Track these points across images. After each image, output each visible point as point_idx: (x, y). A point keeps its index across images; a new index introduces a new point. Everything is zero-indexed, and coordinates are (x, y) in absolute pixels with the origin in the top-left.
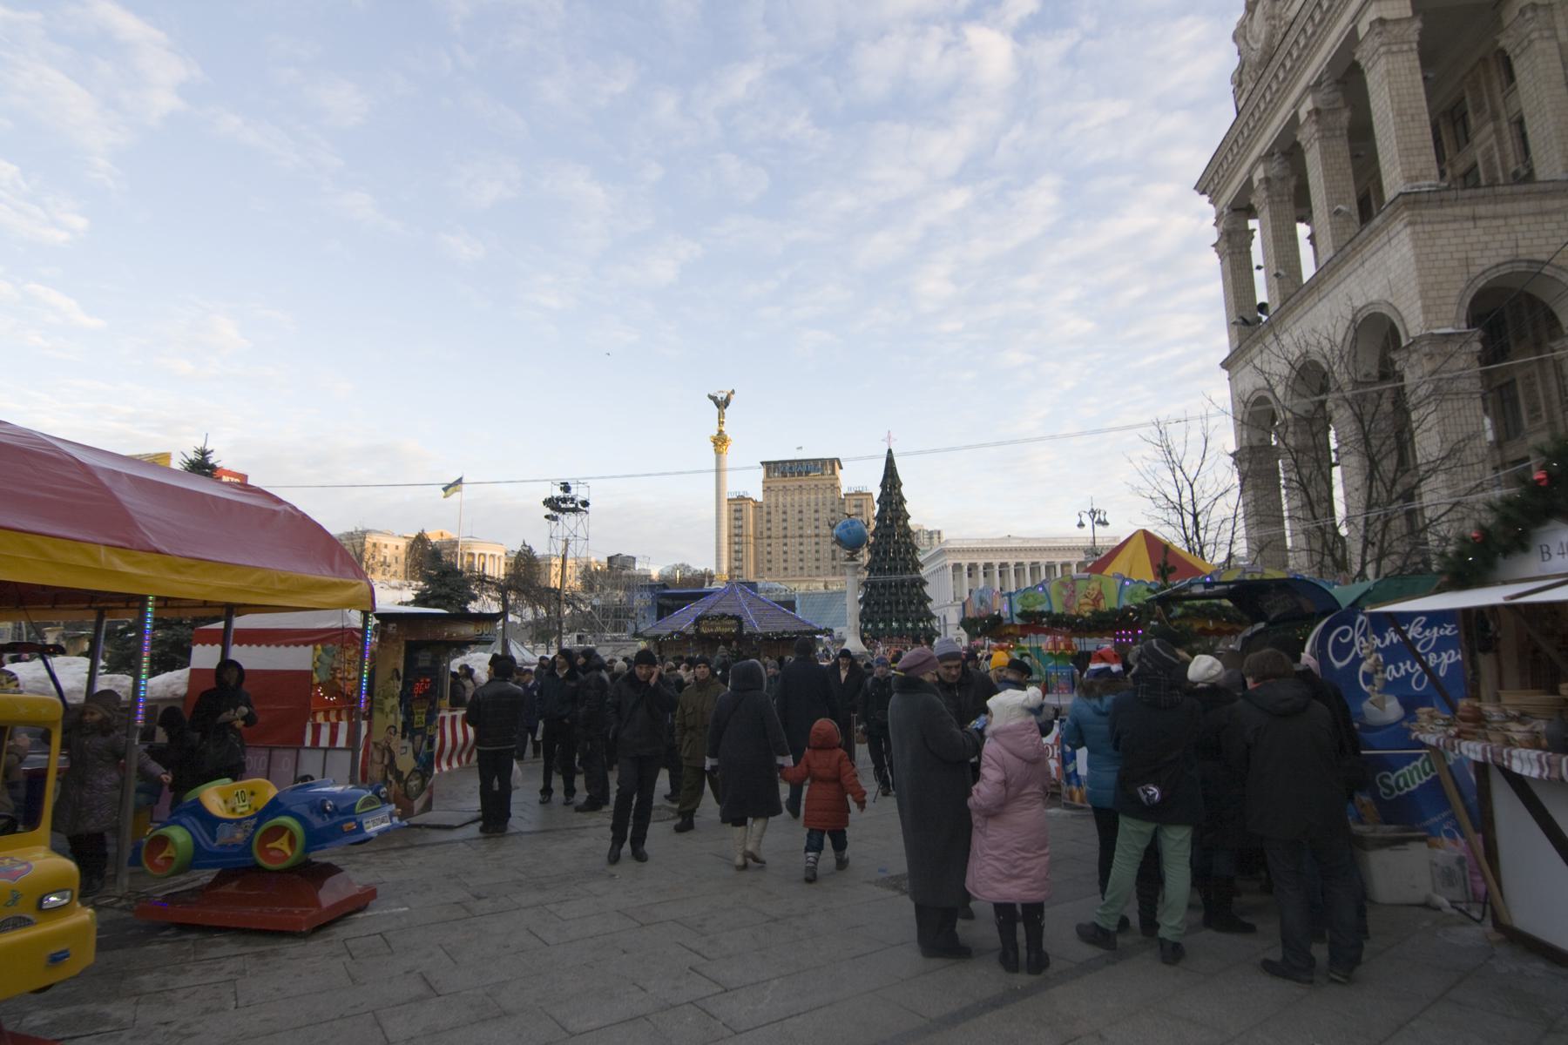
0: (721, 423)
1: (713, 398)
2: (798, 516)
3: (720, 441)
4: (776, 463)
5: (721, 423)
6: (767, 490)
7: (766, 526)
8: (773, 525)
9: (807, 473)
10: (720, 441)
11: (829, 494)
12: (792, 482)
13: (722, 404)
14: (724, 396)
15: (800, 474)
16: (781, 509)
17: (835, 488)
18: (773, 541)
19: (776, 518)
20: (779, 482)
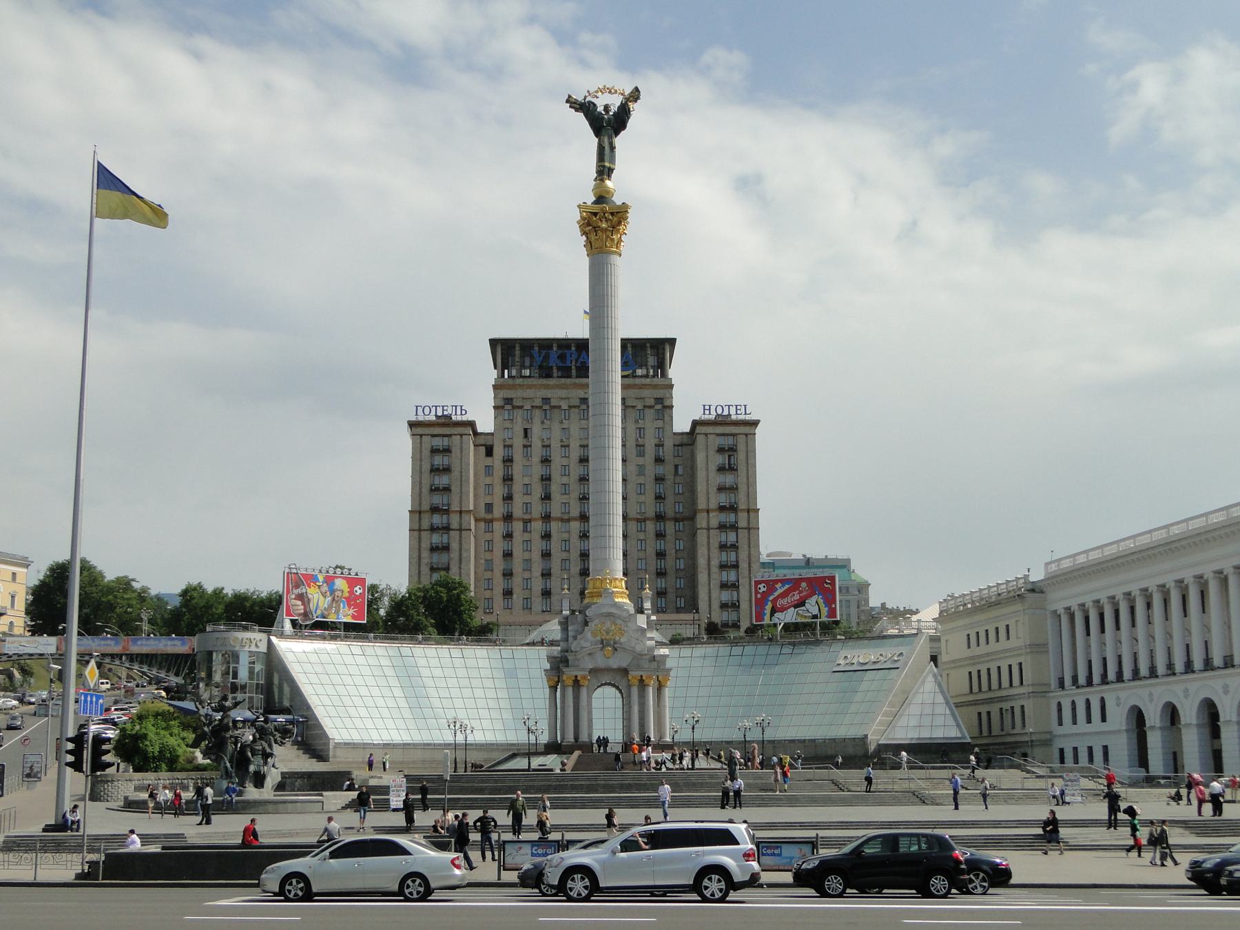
0: (604, 171)
1: (586, 108)
2: (576, 470)
3: (603, 223)
4: (527, 345)
5: (604, 171)
6: (504, 406)
7: (499, 490)
8: (517, 488)
10: (603, 223)
11: (650, 425)
13: (608, 125)
14: (615, 102)
16: (537, 452)
17: (663, 407)
18: (517, 527)
19: (526, 473)
20: (536, 390)
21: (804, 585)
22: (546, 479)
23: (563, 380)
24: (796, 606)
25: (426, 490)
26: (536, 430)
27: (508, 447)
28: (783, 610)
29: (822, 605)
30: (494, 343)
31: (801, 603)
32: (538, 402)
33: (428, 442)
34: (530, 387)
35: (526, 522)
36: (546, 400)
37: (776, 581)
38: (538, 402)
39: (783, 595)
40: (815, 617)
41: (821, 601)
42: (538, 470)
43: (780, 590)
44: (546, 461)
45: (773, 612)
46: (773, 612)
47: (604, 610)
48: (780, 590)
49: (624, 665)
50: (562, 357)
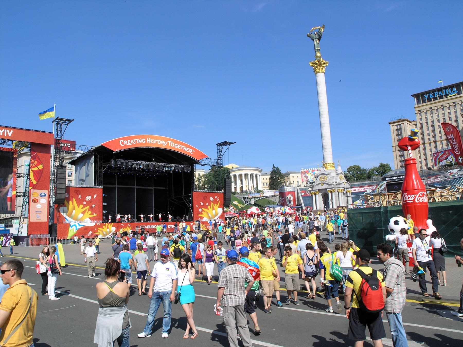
4: (422, 94)
8: (426, 134)
9: (446, 95)
12: (435, 105)
15: (441, 97)
16: (430, 123)
21: (447, 152)
22: (433, 131)
23: (435, 101)
24: (445, 159)
25: (396, 140)
26: (429, 117)
27: (421, 124)
28: (442, 161)
29: (453, 158)
30: (413, 96)
31: (447, 158)
32: (428, 109)
33: (396, 127)
34: (425, 105)
35: (430, 144)
36: (431, 108)
37: (439, 153)
38: (428, 109)
39: (441, 156)
40: (451, 162)
41: (452, 157)
42: (431, 129)
43: (440, 155)
44: (433, 126)
45: (439, 162)
46: (439, 162)
47: (322, 173)
48: (440, 155)
49: (326, 188)
50: (434, 95)
